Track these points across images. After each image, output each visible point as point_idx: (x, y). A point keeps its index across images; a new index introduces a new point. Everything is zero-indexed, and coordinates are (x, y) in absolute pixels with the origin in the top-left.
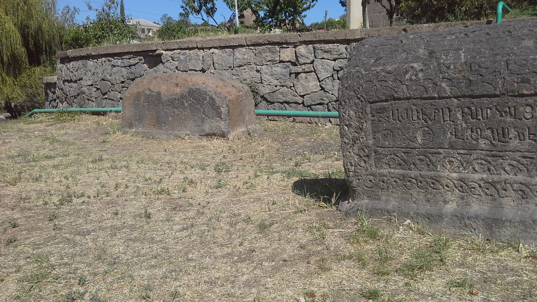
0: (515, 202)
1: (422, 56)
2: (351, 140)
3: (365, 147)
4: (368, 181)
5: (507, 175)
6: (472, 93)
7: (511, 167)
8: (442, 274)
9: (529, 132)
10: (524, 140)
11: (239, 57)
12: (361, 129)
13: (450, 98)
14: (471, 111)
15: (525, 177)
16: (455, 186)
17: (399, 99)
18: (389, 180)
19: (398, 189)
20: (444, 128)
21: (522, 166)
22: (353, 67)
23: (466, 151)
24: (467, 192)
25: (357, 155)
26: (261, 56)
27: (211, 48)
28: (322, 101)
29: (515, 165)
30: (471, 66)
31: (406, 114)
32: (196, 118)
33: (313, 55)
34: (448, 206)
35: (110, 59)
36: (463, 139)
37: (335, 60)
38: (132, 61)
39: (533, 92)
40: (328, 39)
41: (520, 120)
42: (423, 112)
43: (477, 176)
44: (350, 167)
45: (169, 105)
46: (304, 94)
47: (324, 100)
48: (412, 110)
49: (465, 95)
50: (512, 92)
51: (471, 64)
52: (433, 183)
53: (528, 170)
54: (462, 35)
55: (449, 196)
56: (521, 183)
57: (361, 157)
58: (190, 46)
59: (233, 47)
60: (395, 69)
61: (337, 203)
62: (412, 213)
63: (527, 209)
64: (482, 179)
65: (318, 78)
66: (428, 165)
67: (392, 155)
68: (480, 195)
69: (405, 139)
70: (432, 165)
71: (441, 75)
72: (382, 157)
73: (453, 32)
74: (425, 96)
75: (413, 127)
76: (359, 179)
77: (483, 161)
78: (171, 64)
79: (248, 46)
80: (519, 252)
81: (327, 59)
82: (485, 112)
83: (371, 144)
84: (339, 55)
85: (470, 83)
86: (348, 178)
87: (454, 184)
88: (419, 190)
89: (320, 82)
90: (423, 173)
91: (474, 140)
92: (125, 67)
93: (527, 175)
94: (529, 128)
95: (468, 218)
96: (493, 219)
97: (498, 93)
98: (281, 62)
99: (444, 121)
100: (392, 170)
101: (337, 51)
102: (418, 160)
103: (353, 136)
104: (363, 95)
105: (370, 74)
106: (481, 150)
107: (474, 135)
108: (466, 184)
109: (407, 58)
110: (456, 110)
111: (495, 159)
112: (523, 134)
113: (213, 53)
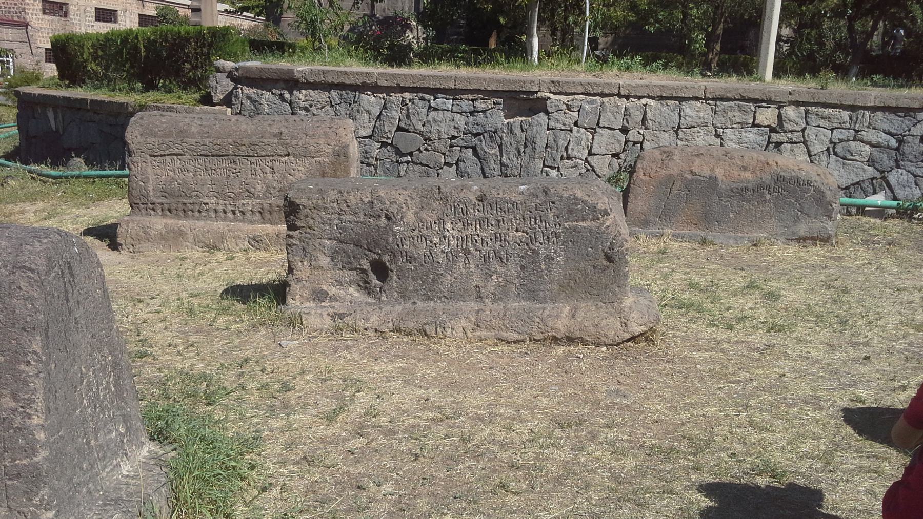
11: (690, 113)
26: (724, 115)
27: (644, 97)
32: (784, 217)
35: (427, 96)
38: (480, 105)
40: (830, 102)
45: (733, 196)
58: (607, 91)
59: (681, 99)
65: (809, 152)
78: (567, 115)
79: (706, 99)
81: (823, 127)
84: (840, 123)
89: (810, 156)
92: (461, 113)
98: (754, 125)
101: (838, 119)
113: (645, 105)
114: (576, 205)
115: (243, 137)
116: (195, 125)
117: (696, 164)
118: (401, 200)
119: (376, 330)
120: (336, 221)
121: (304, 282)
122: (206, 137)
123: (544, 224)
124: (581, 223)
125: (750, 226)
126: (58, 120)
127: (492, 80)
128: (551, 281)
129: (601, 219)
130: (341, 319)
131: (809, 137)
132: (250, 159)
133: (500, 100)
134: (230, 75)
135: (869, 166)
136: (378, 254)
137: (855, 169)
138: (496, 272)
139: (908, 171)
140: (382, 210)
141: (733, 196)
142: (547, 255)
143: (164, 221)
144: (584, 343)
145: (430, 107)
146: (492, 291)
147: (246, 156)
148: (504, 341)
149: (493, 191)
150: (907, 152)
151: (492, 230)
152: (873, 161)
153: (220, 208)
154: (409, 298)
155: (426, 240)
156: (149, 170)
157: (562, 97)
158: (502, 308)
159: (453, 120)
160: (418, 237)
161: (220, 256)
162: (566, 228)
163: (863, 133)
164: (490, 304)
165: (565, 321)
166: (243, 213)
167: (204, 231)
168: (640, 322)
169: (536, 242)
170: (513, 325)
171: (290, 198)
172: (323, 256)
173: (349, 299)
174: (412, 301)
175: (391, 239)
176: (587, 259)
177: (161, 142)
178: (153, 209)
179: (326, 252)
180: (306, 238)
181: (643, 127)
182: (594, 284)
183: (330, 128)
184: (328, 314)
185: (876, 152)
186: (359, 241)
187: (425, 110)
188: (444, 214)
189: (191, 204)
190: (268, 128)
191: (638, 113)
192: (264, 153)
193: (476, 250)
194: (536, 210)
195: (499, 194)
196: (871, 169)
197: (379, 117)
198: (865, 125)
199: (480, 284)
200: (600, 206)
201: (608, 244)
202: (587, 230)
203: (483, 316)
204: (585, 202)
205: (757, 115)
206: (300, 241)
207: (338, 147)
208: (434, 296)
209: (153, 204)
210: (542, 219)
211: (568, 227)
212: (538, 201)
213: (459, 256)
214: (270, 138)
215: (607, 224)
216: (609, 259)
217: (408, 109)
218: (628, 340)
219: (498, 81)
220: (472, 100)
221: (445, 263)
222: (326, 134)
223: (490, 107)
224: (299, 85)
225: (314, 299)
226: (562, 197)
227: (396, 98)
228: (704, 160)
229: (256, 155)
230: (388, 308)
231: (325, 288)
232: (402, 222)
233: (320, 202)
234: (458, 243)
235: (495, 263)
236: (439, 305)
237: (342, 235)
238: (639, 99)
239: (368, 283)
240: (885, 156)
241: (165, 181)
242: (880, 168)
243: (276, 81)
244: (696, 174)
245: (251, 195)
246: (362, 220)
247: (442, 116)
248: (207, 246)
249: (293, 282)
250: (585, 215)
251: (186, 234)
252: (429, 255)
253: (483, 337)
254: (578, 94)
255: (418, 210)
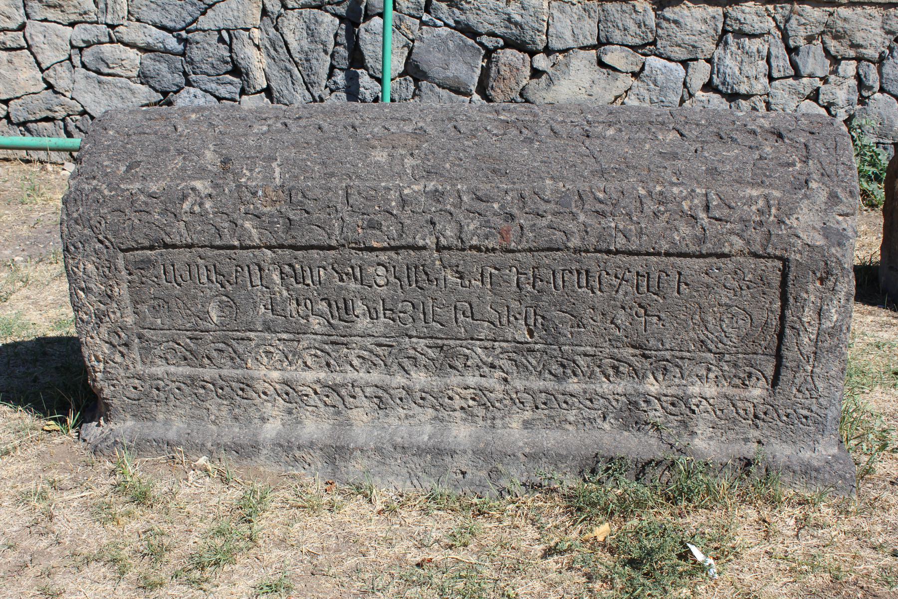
0: (369, 414)
1: (209, 167)
2: (93, 315)
3: (120, 330)
4: (132, 389)
5: (356, 373)
6: (294, 241)
7: (361, 361)
8: (250, 567)
9: (383, 307)
10: (377, 319)
12: (109, 297)
13: (259, 247)
14: (294, 270)
15: (381, 375)
16: (277, 393)
17: (174, 246)
18: (168, 385)
19: (184, 401)
20: (253, 299)
21: (377, 359)
22: (86, 179)
23: (291, 336)
24: (296, 403)
25: (107, 342)
28: (50, 114)
29: (367, 357)
30: (290, 194)
31: (188, 273)
33: (22, 11)
34: (268, 426)
36: (285, 317)
37: (72, 24)
39: (386, 244)
41: (370, 287)
42: (217, 270)
43: (310, 376)
44: (96, 363)
46: (8, 97)
47: (56, 112)
48: (198, 266)
49: (283, 245)
50: (356, 243)
51: (290, 190)
52: (242, 390)
53: (386, 365)
54: (279, 125)
55: (268, 409)
56: (376, 386)
57: (114, 346)
60: (164, 189)
61: (78, 425)
62: (209, 444)
63: (386, 426)
64: (318, 381)
65: (39, 64)
66: (232, 359)
67: (171, 343)
68: (316, 407)
69: (190, 316)
70: (237, 359)
71: (243, 207)
72: (152, 345)
73: (264, 116)
74: (218, 242)
75: (202, 294)
76: (114, 386)
77: (317, 351)
80: (371, 503)
81: (55, 22)
82: (315, 273)
83: (131, 323)
84: (81, 15)
85: (290, 225)
86: (93, 384)
87: (275, 389)
88: (220, 401)
89: (42, 71)
90: (225, 372)
91: (303, 318)
93: (385, 372)
94: (383, 300)
95: (299, 448)
96: (336, 446)
97: (334, 243)
99: (253, 286)
100: (172, 369)
101: (75, 7)
102: (215, 350)
103: (97, 309)
104: (108, 237)
105: (118, 196)
106: (314, 334)
107: (302, 309)
108: (294, 389)
109: (183, 169)
110: (271, 268)
111: (336, 347)
112: (375, 309)
131: (32, 39)
135: (142, 83)
137: (118, 91)
139: (206, 91)
150: (196, 59)
152: (145, 77)
163: (120, 29)
185: (148, 60)
196: (145, 88)
198: (121, 15)
240: (163, 67)
242: (158, 87)
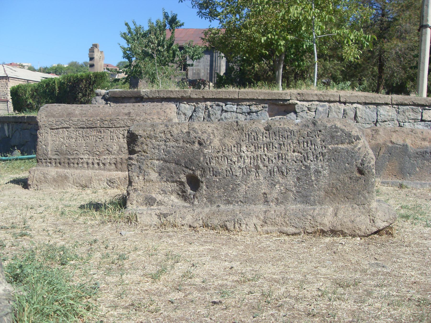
11: (383, 113)
26: (404, 114)
27: (354, 103)
35: (221, 104)
38: (254, 108)
45: (418, 157)
58: (332, 99)
59: (377, 104)
78: (308, 114)
79: (392, 104)
92: (242, 113)
98: (422, 120)
113: (356, 108)
114: (336, 132)
115: (106, 116)
116: (78, 110)
117: (393, 137)
118: (210, 130)
119: (190, 226)
120: (163, 147)
121: (139, 192)
122: (84, 117)
123: (313, 146)
124: (340, 146)
125: (429, 176)
126: (9, 130)
127: (261, 93)
128: (319, 189)
129: (355, 143)
130: (165, 218)
132: (110, 129)
133: (266, 105)
134: (104, 98)
136: (193, 170)
138: (278, 182)
140: (196, 138)
141: (418, 157)
142: (316, 169)
143: (56, 170)
144: (344, 235)
145: (223, 110)
146: (276, 197)
147: (107, 128)
148: (285, 234)
149: (276, 123)
151: (276, 151)
153: (90, 161)
154: (215, 202)
155: (227, 159)
156: (49, 138)
157: (305, 103)
158: (283, 209)
159: (237, 118)
160: (222, 157)
161: (89, 191)
162: (329, 149)
164: (274, 206)
165: (330, 218)
166: (104, 164)
167: (80, 176)
168: (383, 219)
169: (308, 159)
170: (291, 221)
171: (131, 131)
172: (154, 172)
173: (171, 204)
174: (217, 204)
175: (202, 159)
176: (345, 172)
177: (57, 120)
178: (50, 163)
179: (155, 169)
180: (141, 159)
181: (355, 121)
182: (351, 191)
183: (161, 109)
184: (156, 214)
186: (178, 161)
187: (219, 112)
188: (241, 140)
189: (73, 159)
190: (122, 110)
191: (352, 112)
192: (118, 126)
193: (264, 166)
194: (308, 136)
195: (280, 125)
197: (191, 117)
199: (267, 191)
200: (354, 133)
201: (360, 161)
202: (345, 151)
203: (269, 215)
204: (343, 131)
205: (423, 114)
206: (137, 162)
207: (165, 121)
208: (233, 200)
209: (50, 159)
210: (312, 142)
211: (331, 148)
212: (309, 130)
213: (252, 171)
214: (123, 116)
215: (359, 146)
216: (361, 172)
217: (209, 112)
218: (375, 233)
219: (265, 93)
220: (249, 105)
221: (241, 176)
222: (158, 113)
223: (260, 109)
224: (144, 100)
225: (146, 204)
226: (326, 127)
227: (202, 105)
228: (398, 135)
229: (114, 127)
230: (199, 210)
231: (154, 196)
232: (210, 146)
233: (152, 133)
234: (250, 161)
235: (278, 175)
236: (237, 208)
237: (167, 156)
238: (352, 104)
239: (185, 192)
241: (58, 145)
243: (130, 98)
244: (394, 143)
245: (110, 153)
246: (181, 145)
247: (230, 115)
248: (81, 186)
249: (131, 192)
250: (343, 139)
251: (69, 178)
252: (230, 170)
253: (269, 231)
254: (315, 101)
255: (221, 138)
